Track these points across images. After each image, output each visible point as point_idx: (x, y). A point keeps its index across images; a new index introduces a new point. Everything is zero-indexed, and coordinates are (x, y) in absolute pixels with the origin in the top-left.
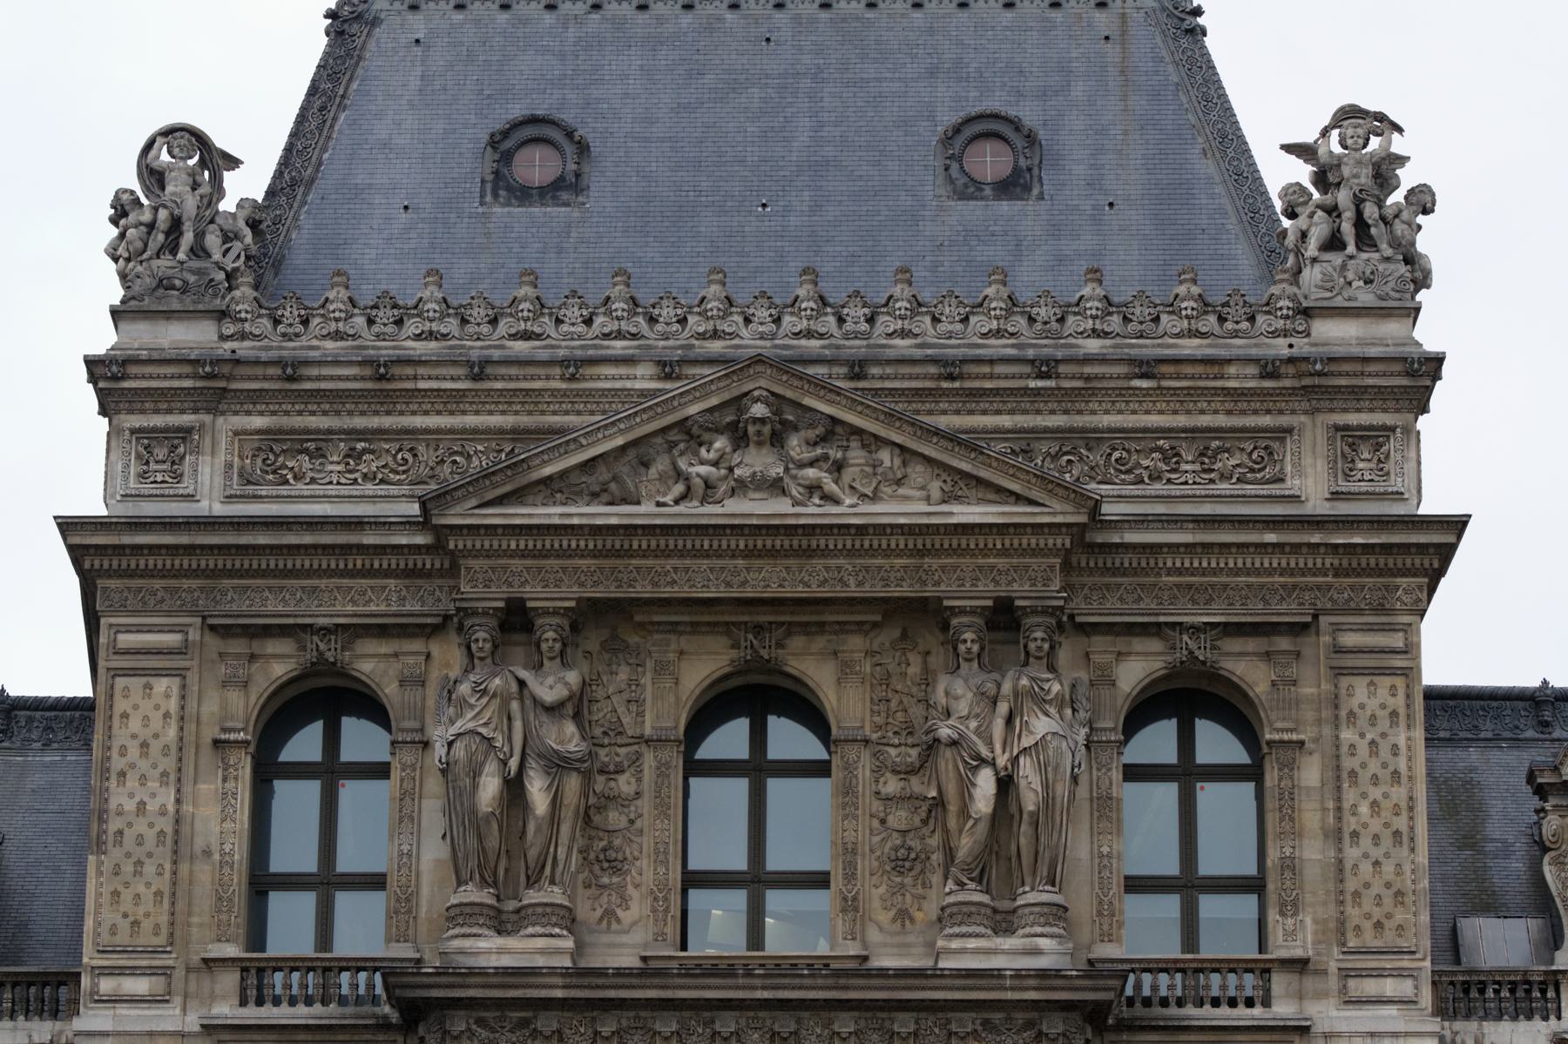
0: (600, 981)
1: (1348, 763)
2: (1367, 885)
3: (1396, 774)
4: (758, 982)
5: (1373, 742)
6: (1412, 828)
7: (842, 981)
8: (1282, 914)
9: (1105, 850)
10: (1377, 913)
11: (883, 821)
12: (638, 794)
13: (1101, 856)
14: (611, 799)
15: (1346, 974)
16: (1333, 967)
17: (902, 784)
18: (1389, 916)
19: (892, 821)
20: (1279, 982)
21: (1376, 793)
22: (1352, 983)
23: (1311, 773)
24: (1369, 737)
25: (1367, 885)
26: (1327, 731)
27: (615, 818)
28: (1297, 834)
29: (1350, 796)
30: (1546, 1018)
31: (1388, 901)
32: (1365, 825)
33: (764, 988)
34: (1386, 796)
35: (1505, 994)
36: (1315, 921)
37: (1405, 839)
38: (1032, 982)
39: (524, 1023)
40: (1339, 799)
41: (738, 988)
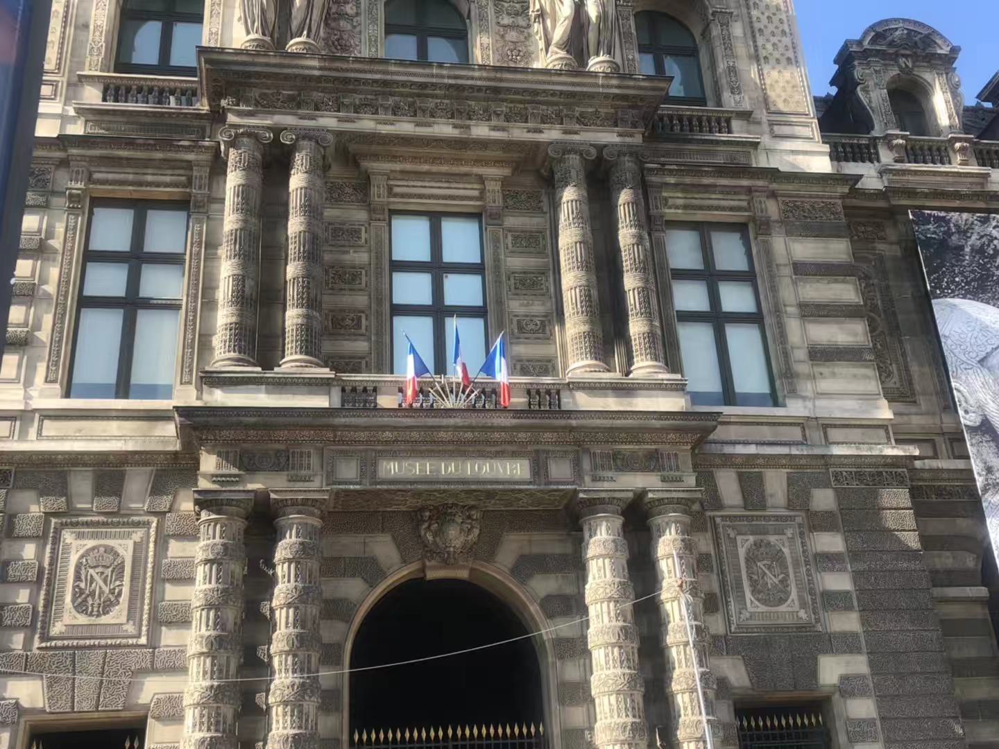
0: (344, 66)
1: (757, 25)
2: (777, 82)
3: (784, 32)
4: (445, 72)
5: (769, 18)
6: (796, 57)
7: (499, 75)
8: (732, 93)
9: (631, 57)
10: (784, 95)
11: (503, 36)
12: (357, 14)
13: (628, 60)
14: (342, 15)
15: (772, 124)
16: (764, 119)
17: (513, 19)
18: (791, 97)
19: (508, 37)
20: (735, 124)
21: (774, 40)
22: (776, 128)
23: (737, 30)
24: (766, 14)
25: (777, 82)
26: (744, 11)
27: (343, 24)
28: (733, 56)
29: (760, 41)
30: (872, 162)
31: (789, 89)
32: (771, 54)
33: (449, 77)
34: (780, 41)
35: (848, 149)
36: (750, 99)
37: (793, 60)
38: (614, 82)
39: (291, 99)
40: (755, 42)
41: (432, 76)
